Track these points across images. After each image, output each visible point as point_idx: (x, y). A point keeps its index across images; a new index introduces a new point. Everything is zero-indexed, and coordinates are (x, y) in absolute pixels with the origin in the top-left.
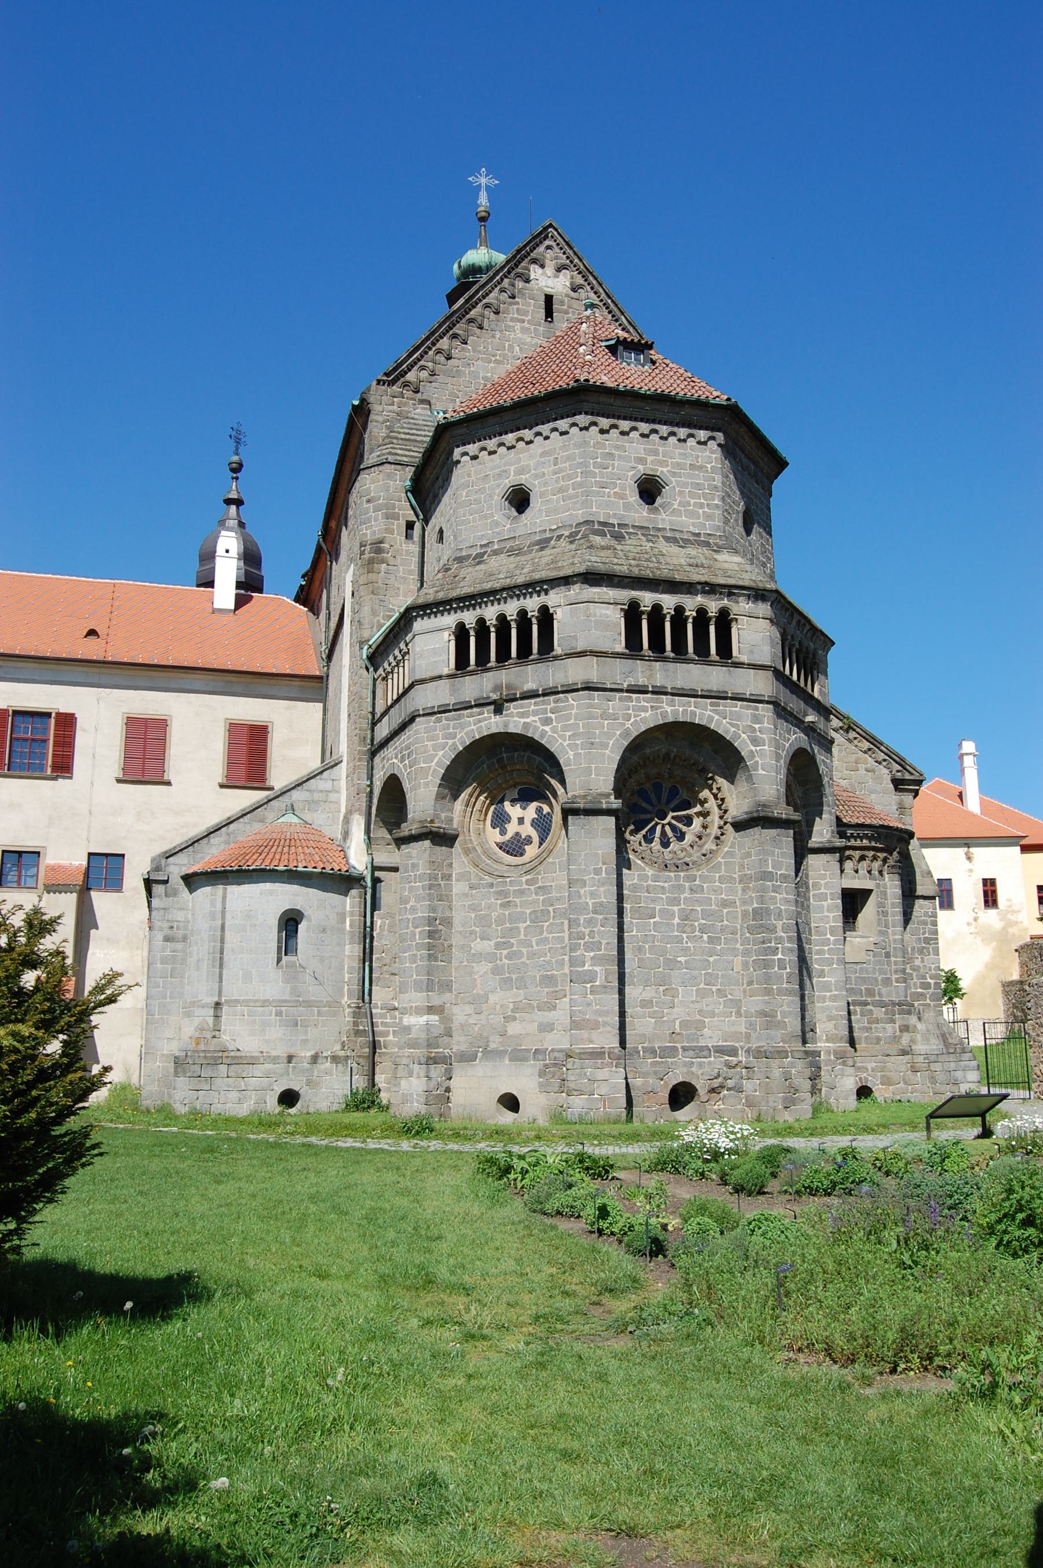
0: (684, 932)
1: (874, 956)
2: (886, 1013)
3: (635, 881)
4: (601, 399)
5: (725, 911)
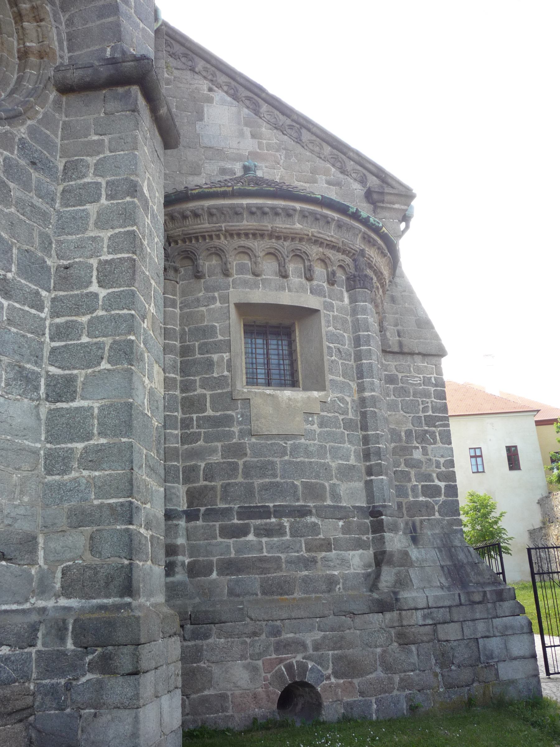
1: (321, 425)
2: (346, 530)
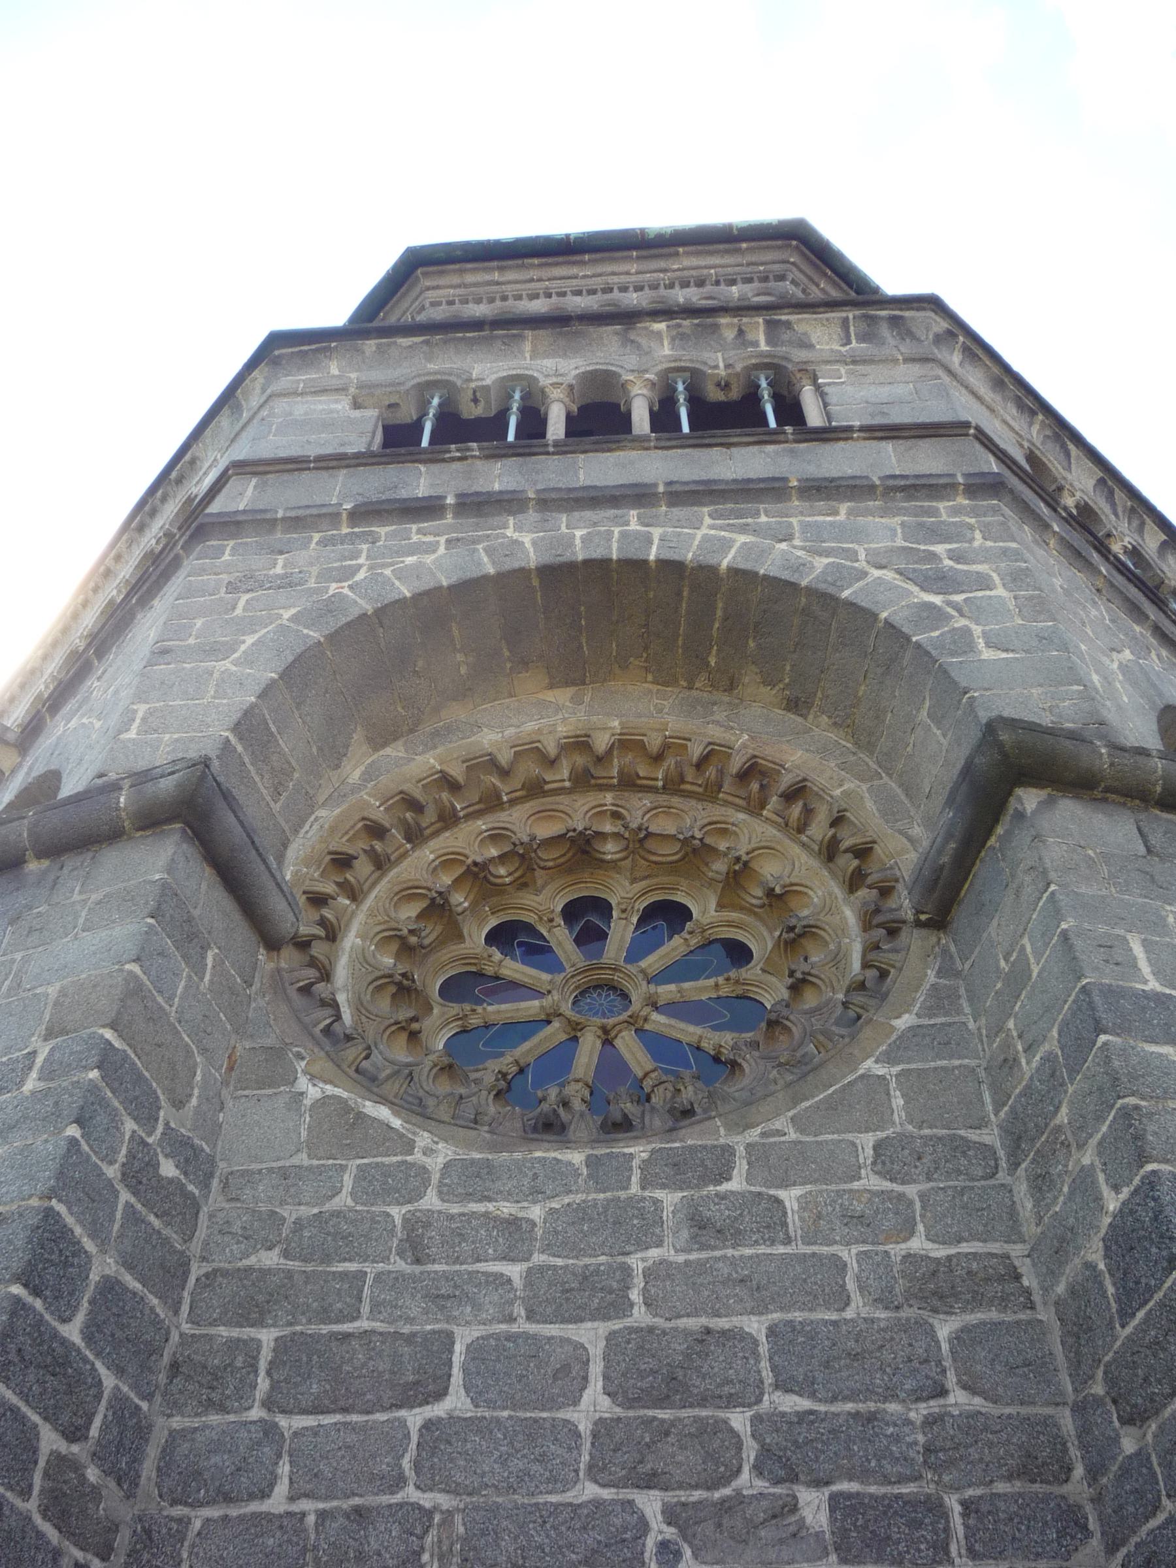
0: (650, 1482)
3: (344, 1200)
4: (470, 278)
5: (945, 1329)
